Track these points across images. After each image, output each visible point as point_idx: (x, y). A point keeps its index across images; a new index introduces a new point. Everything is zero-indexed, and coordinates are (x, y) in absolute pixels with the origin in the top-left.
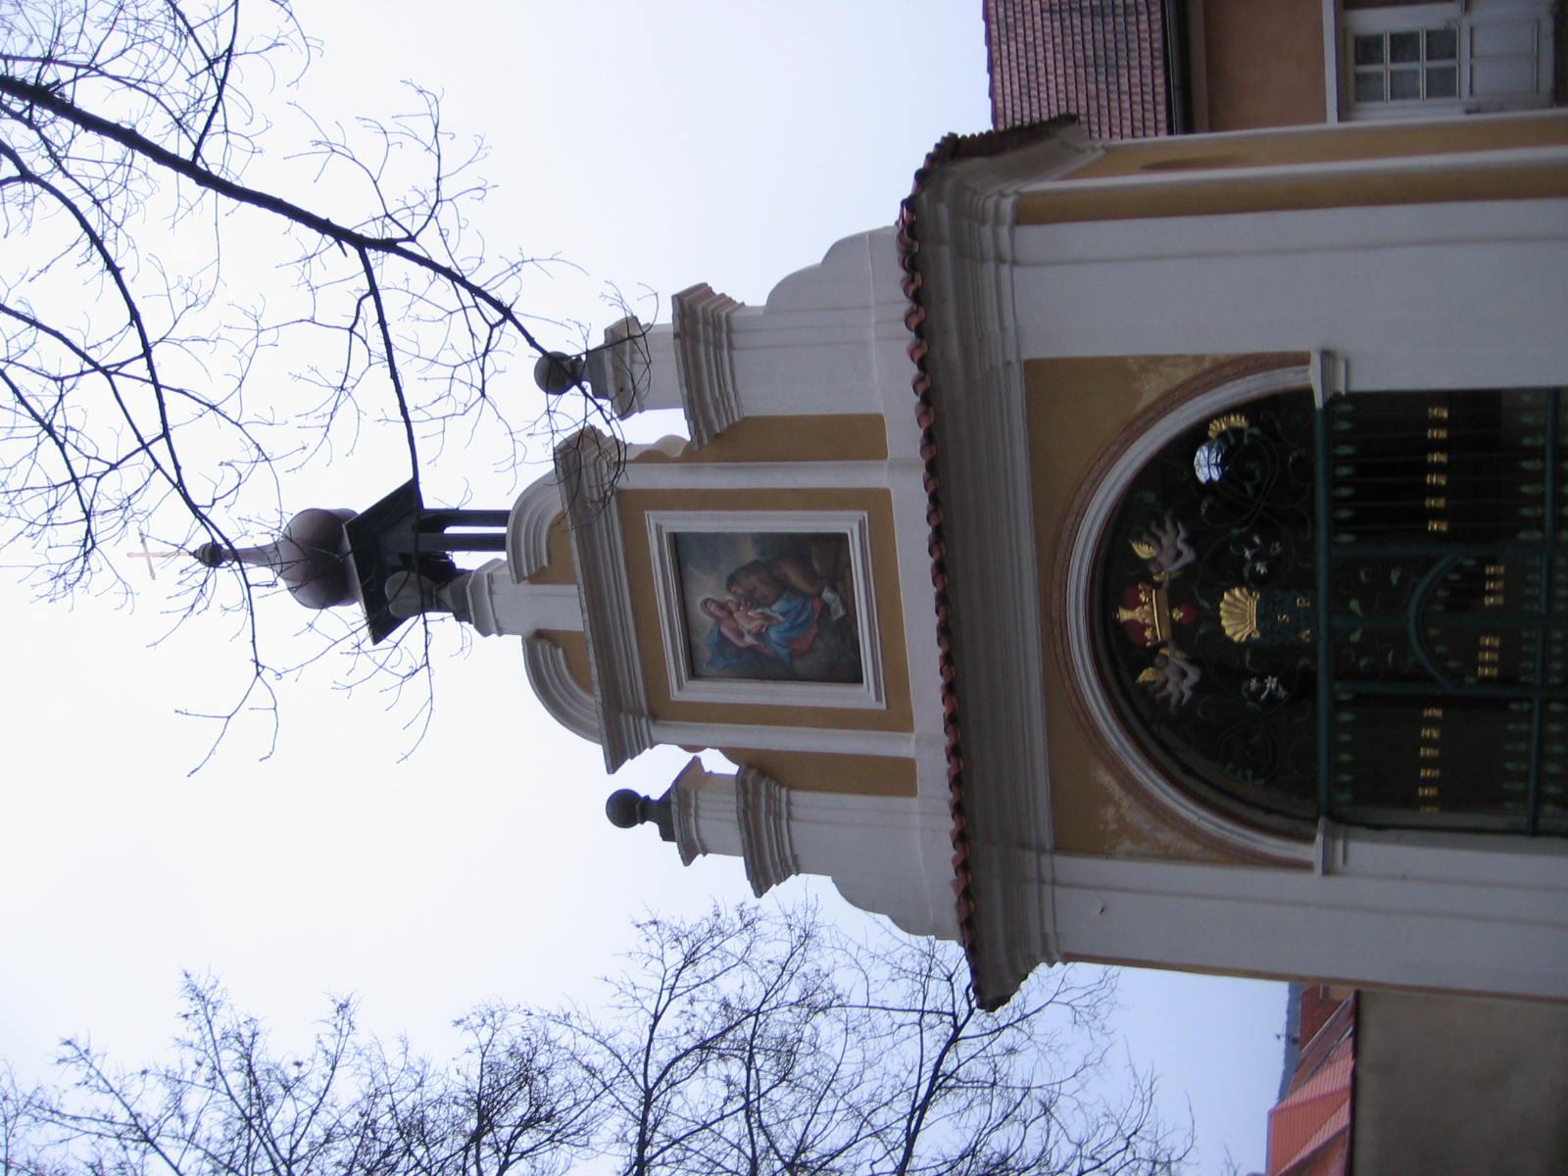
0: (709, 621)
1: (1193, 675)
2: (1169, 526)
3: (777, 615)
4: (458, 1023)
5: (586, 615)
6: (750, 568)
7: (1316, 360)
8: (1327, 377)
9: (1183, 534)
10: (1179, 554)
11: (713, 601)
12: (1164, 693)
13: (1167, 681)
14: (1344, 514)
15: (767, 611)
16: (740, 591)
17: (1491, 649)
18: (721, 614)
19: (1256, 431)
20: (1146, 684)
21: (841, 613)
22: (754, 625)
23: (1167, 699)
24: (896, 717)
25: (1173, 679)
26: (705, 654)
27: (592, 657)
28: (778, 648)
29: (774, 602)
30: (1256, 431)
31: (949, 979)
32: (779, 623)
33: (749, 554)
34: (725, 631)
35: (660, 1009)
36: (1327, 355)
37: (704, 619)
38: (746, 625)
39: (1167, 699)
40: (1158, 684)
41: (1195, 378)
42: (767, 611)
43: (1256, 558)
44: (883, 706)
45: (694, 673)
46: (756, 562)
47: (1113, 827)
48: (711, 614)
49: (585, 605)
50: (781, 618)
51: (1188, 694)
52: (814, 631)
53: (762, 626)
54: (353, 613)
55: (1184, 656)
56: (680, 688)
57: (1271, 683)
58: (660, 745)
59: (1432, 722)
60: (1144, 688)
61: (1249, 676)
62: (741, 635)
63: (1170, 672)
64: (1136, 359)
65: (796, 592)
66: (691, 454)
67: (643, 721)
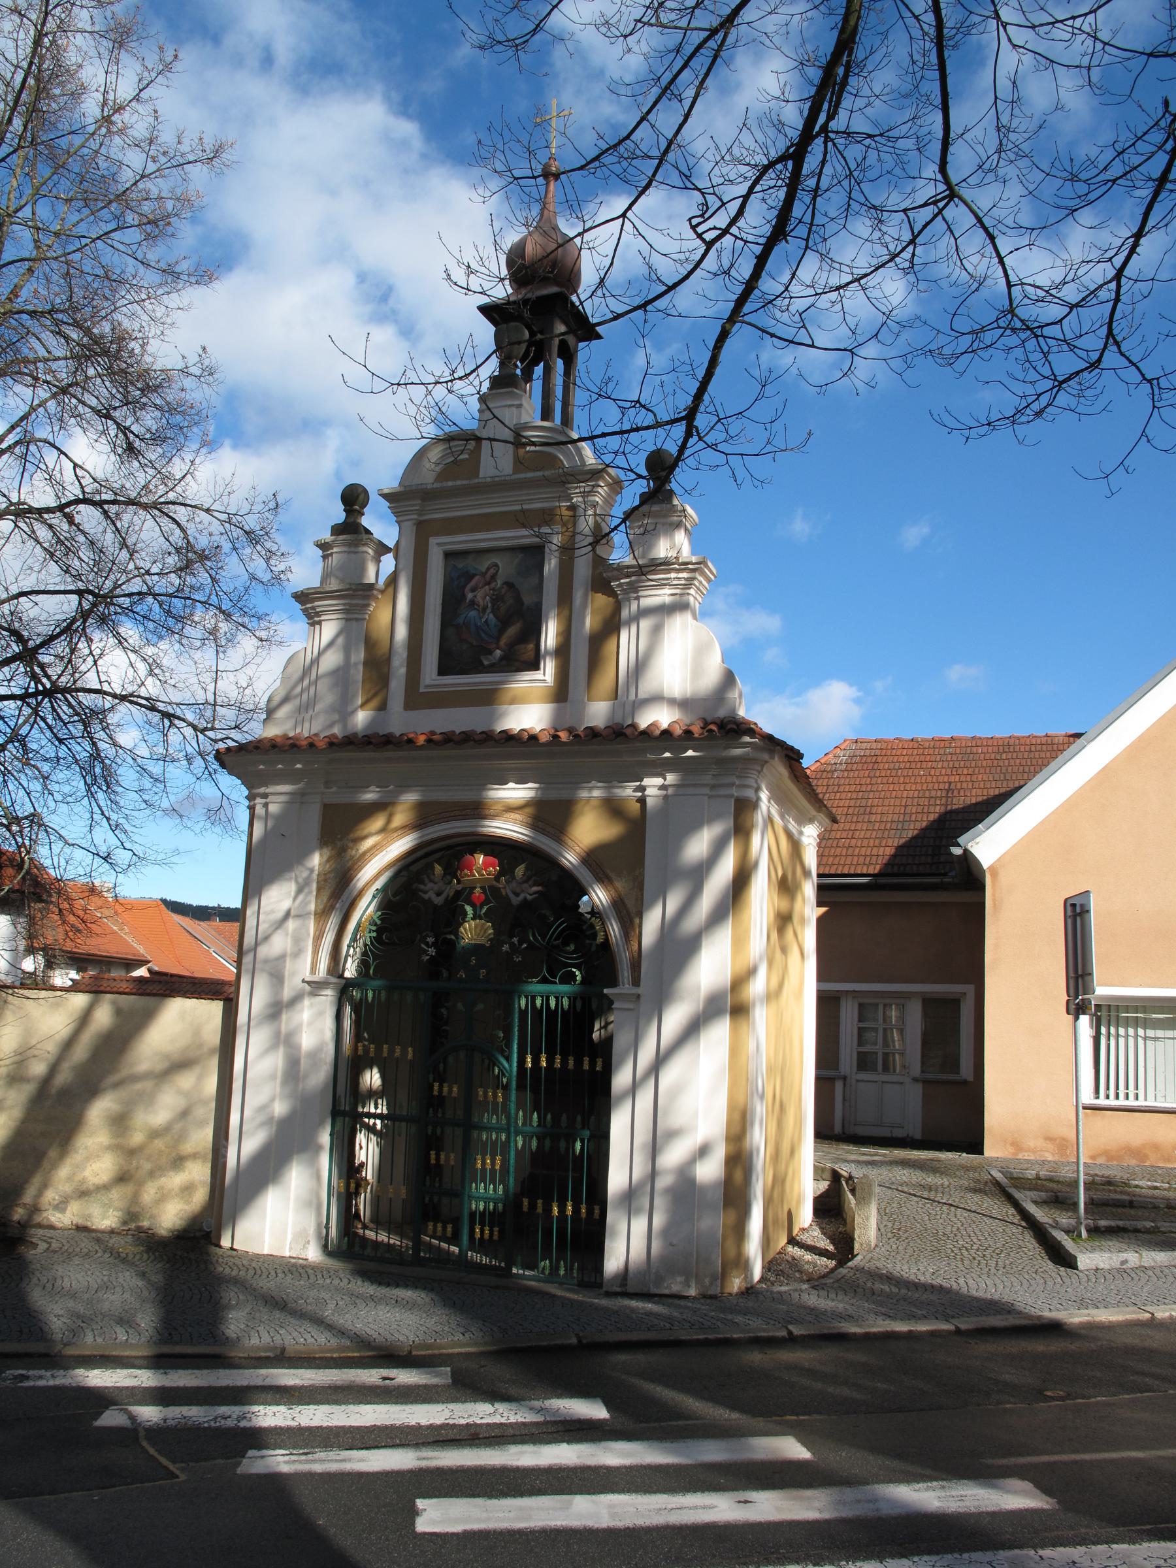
0: (484, 570)
1: (438, 901)
2: (535, 889)
3: (486, 616)
4: (204, 349)
5: (489, 480)
6: (518, 599)
7: (635, 991)
8: (624, 997)
9: (529, 897)
10: (517, 895)
11: (497, 571)
12: (427, 880)
13: (436, 883)
14: (538, 1002)
15: (489, 611)
16: (503, 591)
17: (450, 1091)
19: (594, 948)
20: (433, 869)
21: (486, 663)
22: (479, 600)
23: (423, 882)
24: (416, 699)
25: (436, 887)
26: (461, 564)
27: (459, 483)
28: (463, 616)
29: (495, 616)
30: (594, 948)
31: (237, 727)
32: (481, 618)
33: (528, 600)
34: (477, 578)
35: (215, 514)
36: (638, 996)
37: (484, 564)
38: (480, 594)
39: (423, 882)
40: (432, 877)
41: (628, 911)
42: (489, 611)
43: (512, 945)
44: (422, 690)
45: (448, 555)
46: (523, 604)
47: (339, 844)
48: (488, 569)
49: (496, 479)
50: (483, 620)
51: (426, 897)
52: (475, 643)
53: (479, 606)
54: (502, 292)
55: (451, 895)
56: (439, 544)
57: (432, 951)
59: (404, 1052)
60: (430, 867)
61: (436, 937)
62: (473, 590)
64: (643, 874)
65: (501, 632)
66: (599, 562)
67: (415, 517)
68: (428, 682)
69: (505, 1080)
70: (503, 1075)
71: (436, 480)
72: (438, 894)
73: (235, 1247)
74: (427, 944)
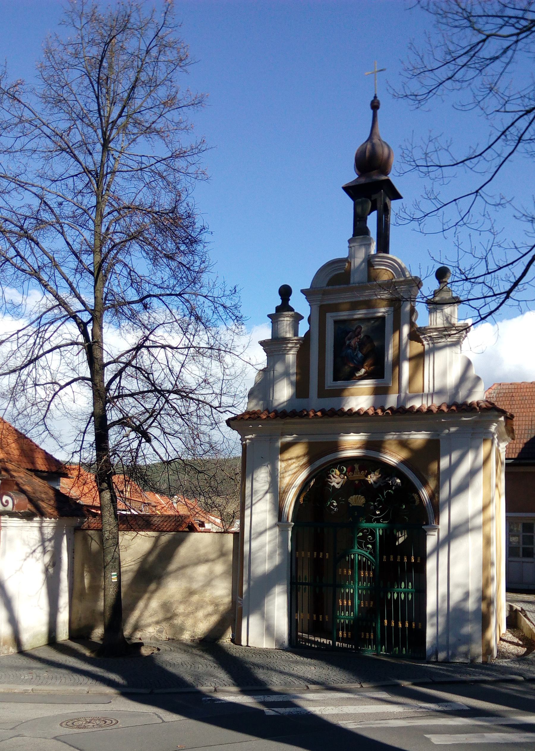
0: (354, 329)
1: (337, 486)
9: (382, 485)
12: (332, 477)
18: (356, 333)
25: (337, 481)
38: (353, 342)
42: (357, 349)
45: (336, 322)
48: (356, 329)
51: (332, 484)
58: (309, 308)
62: (349, 339)
63: (339, 480)
67: (319, 303)
68: (329, 385)
69: (373, 567)
70: (373, 565)
71: (328, 285)
72: (338, 483)
73: (249, 645)
74: (333, 506)
